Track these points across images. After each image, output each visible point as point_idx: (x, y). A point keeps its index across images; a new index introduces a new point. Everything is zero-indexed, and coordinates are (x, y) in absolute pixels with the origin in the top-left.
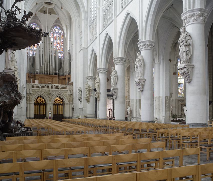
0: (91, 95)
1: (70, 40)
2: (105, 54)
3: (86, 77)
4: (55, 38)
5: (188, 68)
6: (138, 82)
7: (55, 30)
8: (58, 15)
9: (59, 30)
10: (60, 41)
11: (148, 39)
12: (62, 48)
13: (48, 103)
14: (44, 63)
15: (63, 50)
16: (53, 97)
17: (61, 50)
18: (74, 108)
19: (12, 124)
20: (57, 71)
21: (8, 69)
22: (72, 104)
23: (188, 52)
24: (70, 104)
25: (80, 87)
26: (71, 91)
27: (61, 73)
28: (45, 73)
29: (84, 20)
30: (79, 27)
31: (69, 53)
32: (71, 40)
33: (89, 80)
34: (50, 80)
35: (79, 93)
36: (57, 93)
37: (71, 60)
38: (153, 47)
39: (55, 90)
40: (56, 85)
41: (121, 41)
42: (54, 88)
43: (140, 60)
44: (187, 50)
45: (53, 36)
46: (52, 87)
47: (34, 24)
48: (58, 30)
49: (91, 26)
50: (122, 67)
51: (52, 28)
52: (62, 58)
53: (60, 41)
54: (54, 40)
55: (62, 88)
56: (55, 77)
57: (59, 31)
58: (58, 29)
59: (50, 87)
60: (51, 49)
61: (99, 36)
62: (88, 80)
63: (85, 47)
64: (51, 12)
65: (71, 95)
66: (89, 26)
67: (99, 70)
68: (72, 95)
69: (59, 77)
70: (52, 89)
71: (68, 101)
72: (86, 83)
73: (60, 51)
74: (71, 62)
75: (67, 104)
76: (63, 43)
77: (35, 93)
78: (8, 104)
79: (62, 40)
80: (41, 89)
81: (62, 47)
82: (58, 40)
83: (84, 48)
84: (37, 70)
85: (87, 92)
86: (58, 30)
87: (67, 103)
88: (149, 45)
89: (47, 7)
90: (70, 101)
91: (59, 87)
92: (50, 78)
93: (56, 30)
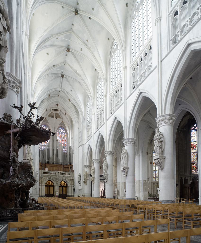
0: (88, 179)
1: (72, 138)
2: (98, 148)
3: (84, 166)
7: (60, 131)
9: (64, 130)
10: (64, 139)
11: (130, 137)
14: (52, 156)
15: (67, 146)
17: (65, 146)
18: (75, 189)
20: (62, 162)
22: (73, 186)
24: (72, 186)
25: (79, 173)
27: (65, 164)
30: (79, 128)
31: (71, 148)
32: (72, 139)
33: (86, 168)
34: (57, 168)
36: (62, 178)
37: (72, 153)
38: (135, 143)
39: (61, 176)
40: (61, 172)
41: (111, 139)
43: (125, 153)
48: (63, 130)
49: (88, 128)
50: (111, 158)
51: (58, 128)
52: (66, 152)
55: (66, 174)
57: (63, 131)
58: (62, 129)
59: (57, 173)
60: (57, 145)
61: (94, 135)
62: (85, 168)
65: (73, 179)
66: (86, 127)
67: (94, 160)
68: (74, 179)
69: (63, 166)
70: (59, 175)
72: (84, 170)
74: (72, 155)
75: (70, 186)
76: (66, 140)
79: (65, 138)
80: (50, 175)
81: (66, 143)
82: (63, 138)
84: (47, 161)
85: (85, 177)
86: (63, 130)
87: (70, 185)
88: (132, 142)
92: (57, 167)
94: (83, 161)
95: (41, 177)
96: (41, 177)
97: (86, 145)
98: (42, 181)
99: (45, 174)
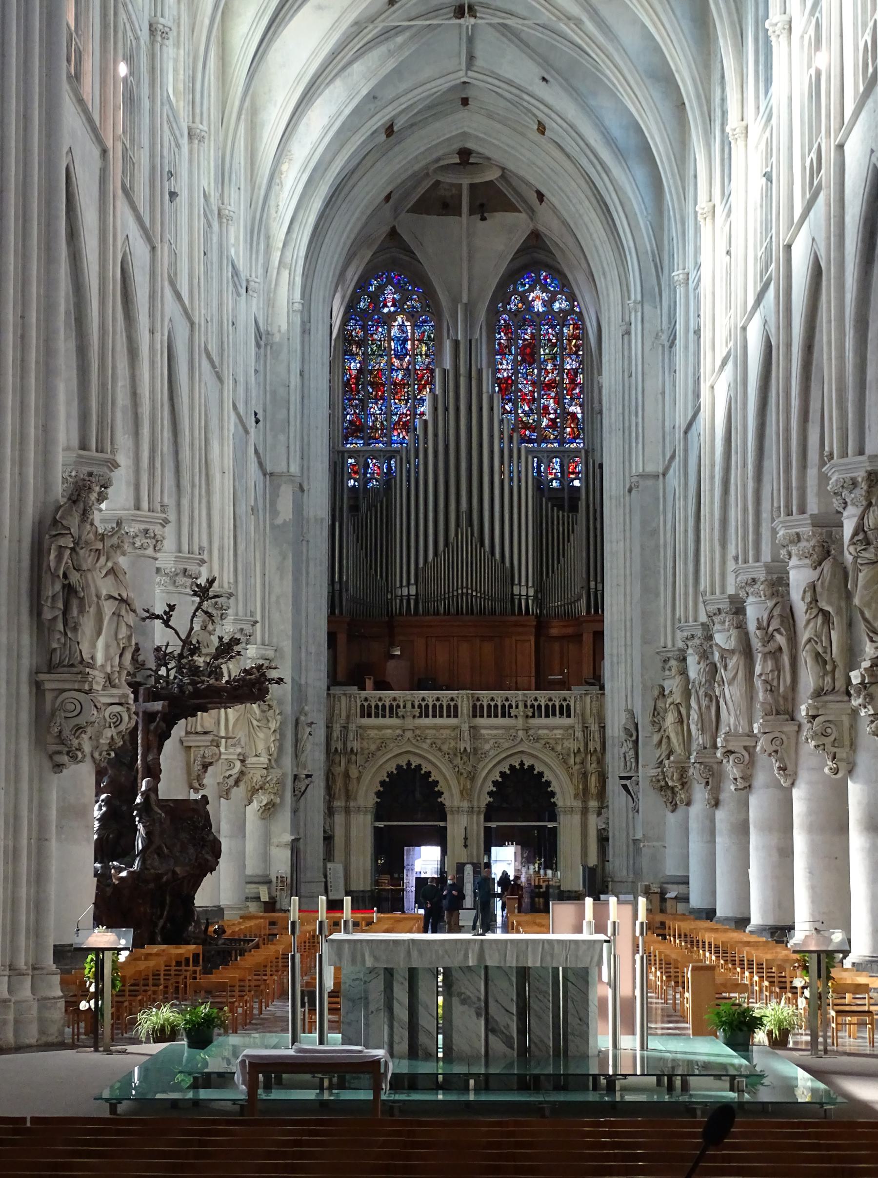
3: (658, 653)
4: (528, 351)
5: (771, 736)
6: (725, 750)
7: (524, 299)
8: (532, 212)
12: (574, 415)
13: (456, 804)
14: (446, 544)
15: (583, 429)
16: (486, 771)
17: (568, 430)
18: (607, 839)
19: (191, 928)
21: (197, 733)
23: (773, 675)
24: (585, 811)
28: (453, 610)
29: (639, 307)
35: (623, 750)
36: (506, 745)
42: (489, 716)
44: (770, 669)
45: (509, 339)
46: (475, 706)
47: (390, 282)
51: (502, 285)
53: (561, 374)
55: (536, 711)
56: (521, 629)
57: (552, 300)
58: (544, 289)
59: (465, 707)
61: (686, 439)
63: (650, 468)
69: (541, 626)
70: (480, 721)
71: (572, 792)
72: (656, 693)
73: (562, 442)
76: (580, 378)
77: (378, 749)
78: (180, 876)
79: (570, 364)
81: (575, 409)
82: (549, 367)
83: (643, 476)
87: (569, 804)
89: (455, 181)
90: (584, 794)
91: (517, 707)
94: (647, 616)
95: (340, 746)
96: (345, 744)
97: (667, 476)
98: (347, 775)
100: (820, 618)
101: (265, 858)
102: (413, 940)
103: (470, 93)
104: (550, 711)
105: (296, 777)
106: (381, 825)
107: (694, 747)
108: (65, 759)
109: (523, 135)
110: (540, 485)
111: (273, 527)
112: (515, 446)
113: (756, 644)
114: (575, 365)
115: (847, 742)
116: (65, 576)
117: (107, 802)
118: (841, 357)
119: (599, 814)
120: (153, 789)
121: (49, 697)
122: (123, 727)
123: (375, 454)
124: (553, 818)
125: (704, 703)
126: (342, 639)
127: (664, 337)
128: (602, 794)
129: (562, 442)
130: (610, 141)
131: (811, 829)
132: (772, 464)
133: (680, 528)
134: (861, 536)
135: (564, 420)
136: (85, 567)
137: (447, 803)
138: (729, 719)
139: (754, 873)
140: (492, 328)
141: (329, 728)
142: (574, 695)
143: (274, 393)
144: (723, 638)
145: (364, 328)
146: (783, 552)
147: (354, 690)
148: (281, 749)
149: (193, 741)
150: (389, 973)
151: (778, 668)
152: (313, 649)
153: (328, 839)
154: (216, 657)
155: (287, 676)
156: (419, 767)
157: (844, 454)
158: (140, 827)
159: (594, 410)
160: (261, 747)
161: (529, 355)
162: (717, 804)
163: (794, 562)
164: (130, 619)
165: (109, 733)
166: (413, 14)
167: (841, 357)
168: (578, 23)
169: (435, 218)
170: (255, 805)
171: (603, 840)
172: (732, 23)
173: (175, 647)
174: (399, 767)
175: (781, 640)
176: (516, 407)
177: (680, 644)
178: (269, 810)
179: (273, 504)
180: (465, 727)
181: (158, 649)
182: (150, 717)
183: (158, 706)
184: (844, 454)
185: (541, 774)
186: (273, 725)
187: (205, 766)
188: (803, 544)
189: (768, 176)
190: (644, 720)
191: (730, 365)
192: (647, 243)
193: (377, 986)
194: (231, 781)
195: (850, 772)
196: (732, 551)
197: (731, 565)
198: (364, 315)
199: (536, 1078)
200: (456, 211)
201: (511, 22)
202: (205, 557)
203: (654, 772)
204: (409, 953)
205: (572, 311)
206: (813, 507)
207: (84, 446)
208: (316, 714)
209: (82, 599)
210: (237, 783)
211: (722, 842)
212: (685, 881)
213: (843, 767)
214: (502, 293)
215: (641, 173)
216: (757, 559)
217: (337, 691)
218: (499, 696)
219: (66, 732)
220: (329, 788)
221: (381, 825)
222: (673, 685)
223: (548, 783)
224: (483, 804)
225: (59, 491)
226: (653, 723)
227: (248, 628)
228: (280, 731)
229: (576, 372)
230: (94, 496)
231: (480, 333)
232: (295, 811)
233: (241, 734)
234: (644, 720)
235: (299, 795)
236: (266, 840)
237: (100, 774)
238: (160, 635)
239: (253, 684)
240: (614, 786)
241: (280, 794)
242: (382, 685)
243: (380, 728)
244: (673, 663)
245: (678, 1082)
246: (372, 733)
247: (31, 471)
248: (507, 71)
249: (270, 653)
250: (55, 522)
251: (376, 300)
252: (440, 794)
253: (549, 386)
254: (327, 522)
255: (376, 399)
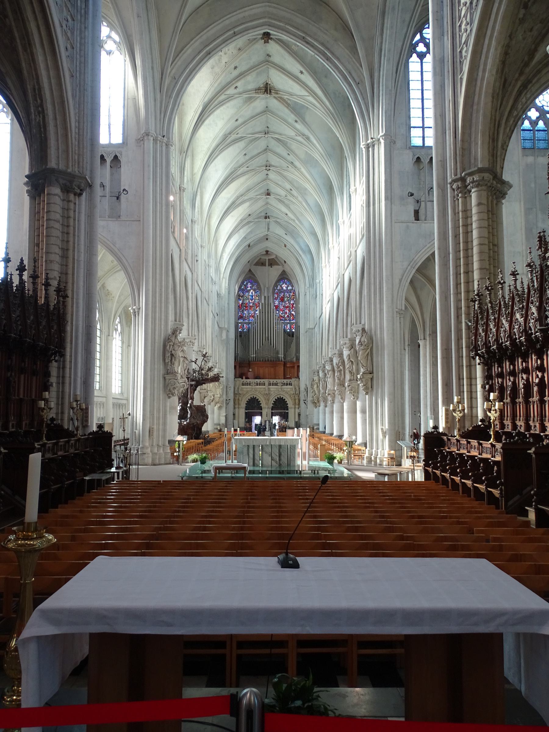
7: (281, 286)
13: (265, 406)
14: (263, 345)
19: (201, 436)
22: (298, 409)
24: (295, 408)
26: (297, 388)
28: (264, 360)
54: (281, 303)
55: (284, 384)
57: (288, 287)
58: (286, 284)
59: (267, 384)
63: (311, 327)
64: (273, 263)
69: (285, 364)
70: (270, 387)
76: (294, 305)
81: (293, 313)
82: (287, 303)
83: (309, 329)
93: (283, 286)
98: (239, 399)
99: (245, 386)
100: (351, 363)
101: (219, 419)
102: (254, 439)
103: (268, 237)
104: (287, 384)
105: (226, 400)
106: (247, 411)
107: (321, 393)
108: (171, 395)
109: (281, 247)
110: (285, 331)
111: (221, 340)
112: (279, 321)
113: (336, 369)
114: (293, 302)
115: (357, 392)
116: (171, 352)
117: (181, 406)
118: (356, 301)
119: (298, 409)
120: (192, 403)
121: (167, 380)
122: (185, 388)
123: (246, 323)
124: (287, 410)
125: (323, 382)
126: (237, 367)
127: (314, 296)
128: (299, 404)
129: (290, 320)
130: (302, 249)
131: (348, 412)
132: (339, 326)
133: (318, 341)
134: (360, 343)
135: (291, 315)
136: (176, 349)
137: (262, 406)
138: (329, 386)
139: (335, 423)
140: (274, 293)
141: (234, 388)
142: (293, 381)
143: (221, 308)
144: (328, 367)
145: (243, 293)
146: (342, 347)
147: (240, 379)
148: (223, 393)
149: (202, 391)
150: (248, 446)
151: (341, 374)
152: (230, 369)
153: (234, 415)
154: (207, 371)
155: (224, 376)
156: (256, 398)
157: (356, 324)
158: (189, 412)
159: (298, 313)
160: (218, 393)
161: (282, 300)
162: (326, 407)
163: (344, 349)
164: (187, 362)
165: (182, 389)
166: (255, 218)
167: (356, 301)
168: (294, 221)
169: (260, 267)
170: (217, 406)
171: (299, 415)
172: (330, 222)
173: (198, 369)
174: (251, 398)
175: (341, 368)
176: (279, 312)
177: (318, 369)
178: (220, 408)
179: (221, 335)
180: (267, 388)
181: (193, 369)
182: (191, 385)
183: (193, 383)
184: (356, 324)
185: (285, 399)
186: (221, 388)
187: (205, 397)
188: (347, 345)
189: (339, 258)
190: (309, 387)
191: (330, 302)
192: (310, 273)
193: (246, 449)
194: (211, 401)
195: (357, 399)
196: (330, 346)
197: (330, 350)
198: (243, 290)
199: (283, 471)
200: (265, 265)
201: (278, 220)
202: (205, 347)
203: (312, 399)
204: (253, 442)
205: (292, 289)
206: (349, 336)
207: (176, 321)
208: (231, 385)
209: (175, 357)
210: (212, 401)
211: (327, 415)
212: (318, 425)
213: (355, 397)
214: (276, 285)
215: (309, 257)
216: (336, 349)
217: (236, 379)
218: (275, 381)
219: (171, 389)
220: (234, 402)
221: (247, 411)
222: (316, 378)
223: (286, 401)
224: (271, 406)
225: (170, 331)
226: (311, 387)
227: (215, 364)
228: (223, 389)
229: (293, 304)
230: (178, 333)
231: (271, 294)
232: (226, 408)
233: (213, 390)
234: (309, 387)
235: (227, 404)
236: (219, 415)
237: (179, 399)
238: (194, 366)
239: (216, 378)
240: (302, 402)
241: (222, 404)
242: (247, 378)
243: (246, 388)
244: (316, 373)
245: (316, 472)
246: (245, 389)
247: (163, 326)
248: (277, 232)
249: (220, 370)
250: (169, 339)
251: (246, 286)
252: (261, 404)
253: (287, 307)
254: (234, 339)
255: (246, 310)
